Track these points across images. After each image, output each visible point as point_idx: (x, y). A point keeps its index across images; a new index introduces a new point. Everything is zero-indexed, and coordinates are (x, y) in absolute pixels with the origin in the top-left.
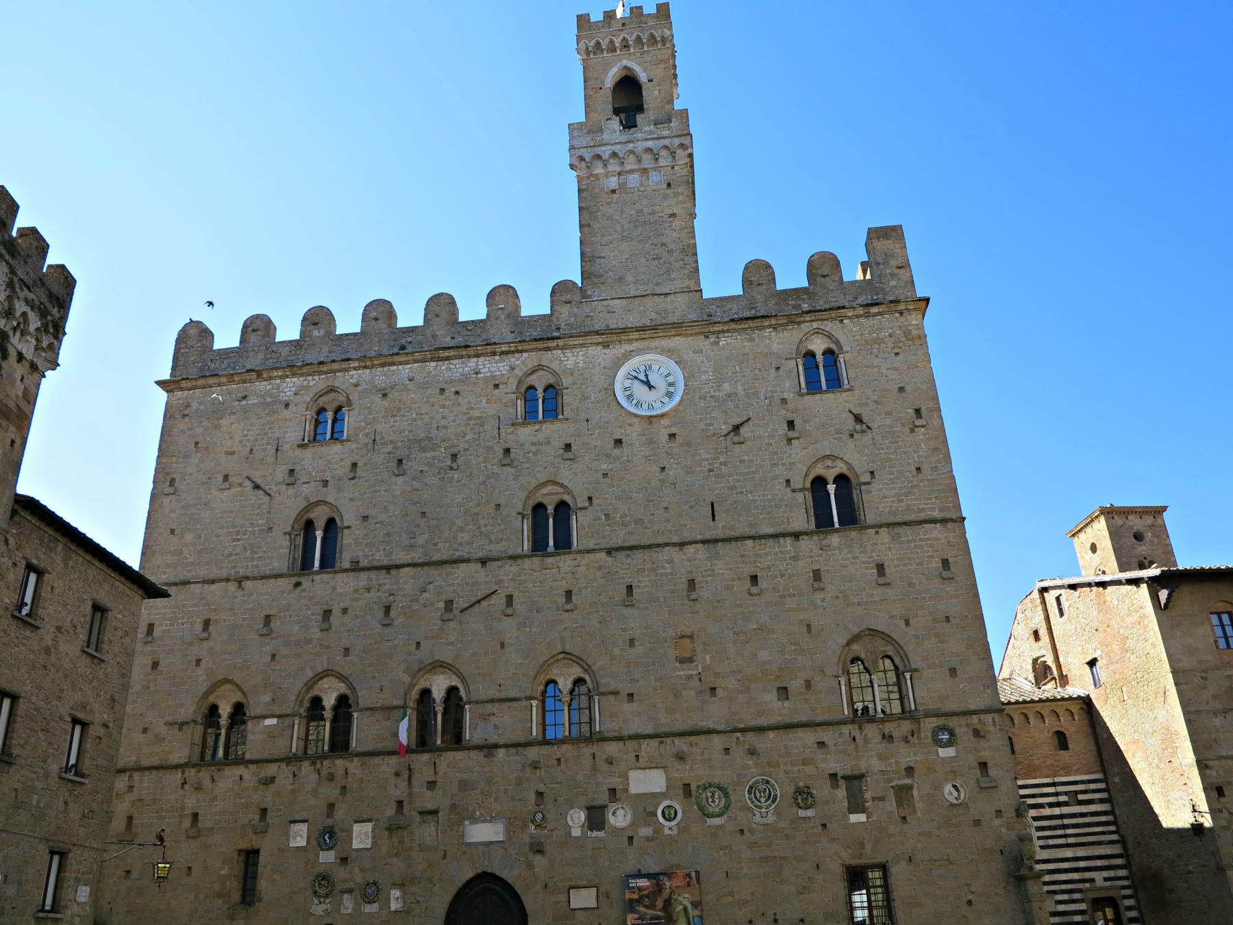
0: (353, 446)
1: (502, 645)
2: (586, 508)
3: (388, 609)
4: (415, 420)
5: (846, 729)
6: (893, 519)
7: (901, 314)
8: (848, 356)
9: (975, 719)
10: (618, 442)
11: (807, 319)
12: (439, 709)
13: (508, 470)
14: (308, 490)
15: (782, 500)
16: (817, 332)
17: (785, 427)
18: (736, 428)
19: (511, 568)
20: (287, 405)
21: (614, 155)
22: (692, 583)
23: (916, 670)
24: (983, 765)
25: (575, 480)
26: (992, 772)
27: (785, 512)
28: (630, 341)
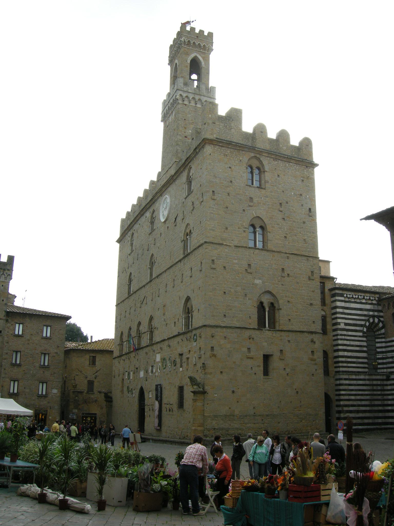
19: (147, 287)
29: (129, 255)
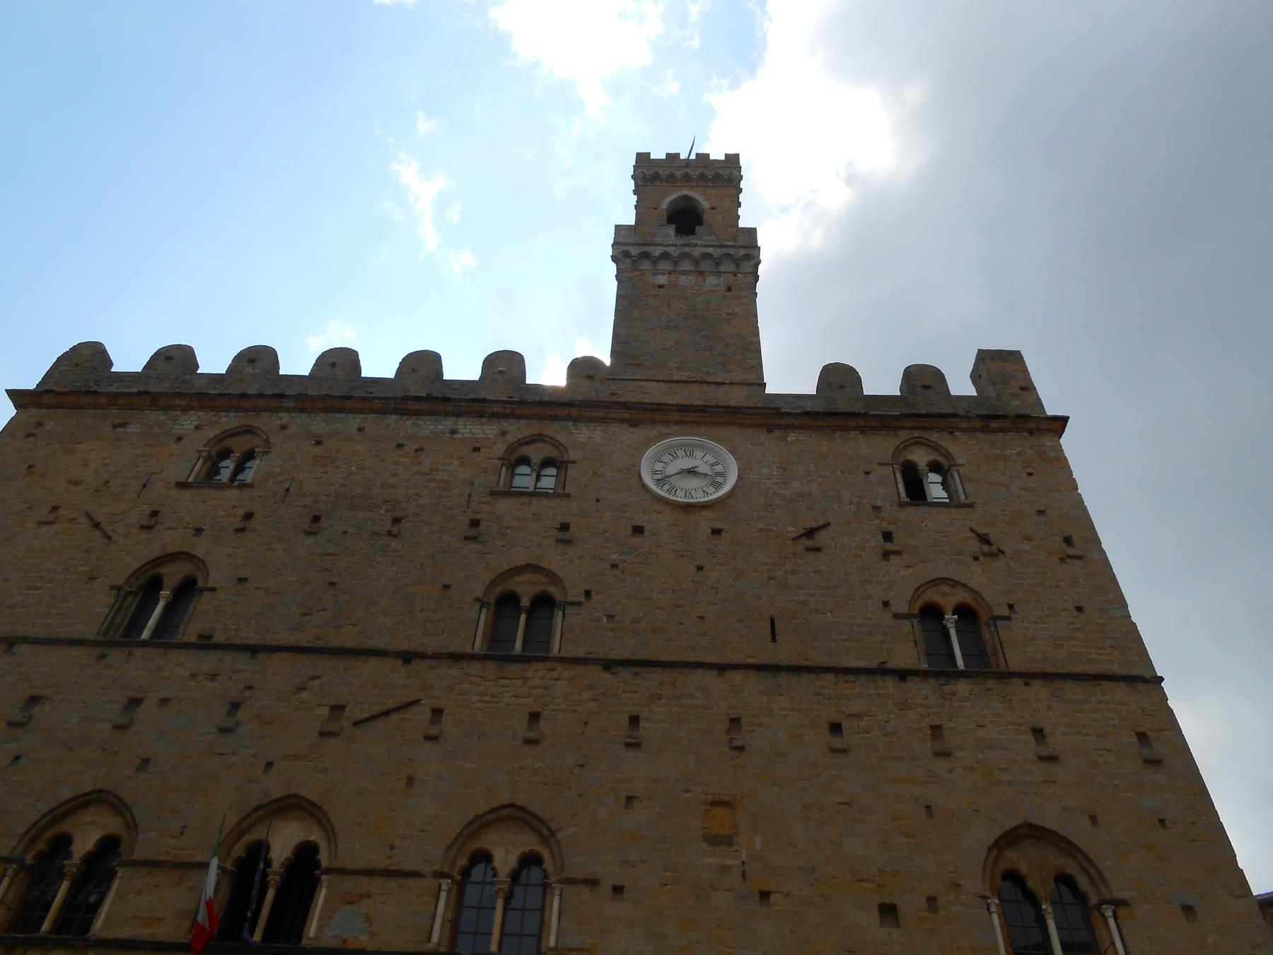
0: (255, 493)
1: (410, 781)
2: (579, 604)
3: (235, 707)
4: (352, 473)
6: (1049, 668)
7: (1031, 433)
8: (962, 470)
10: (638, 530)
11: (907, 424)
12: (274, 879)
13: (474, 546)
14: (168, 539)
16: (918, 442)
17: (880, 537)
18: (810, 533)
19: (452, 672)
20: (180, 439)
21: (665, 256)
22: (735, 722)
25: (571, 568)
28: (666, 423)
29: (182, 485)
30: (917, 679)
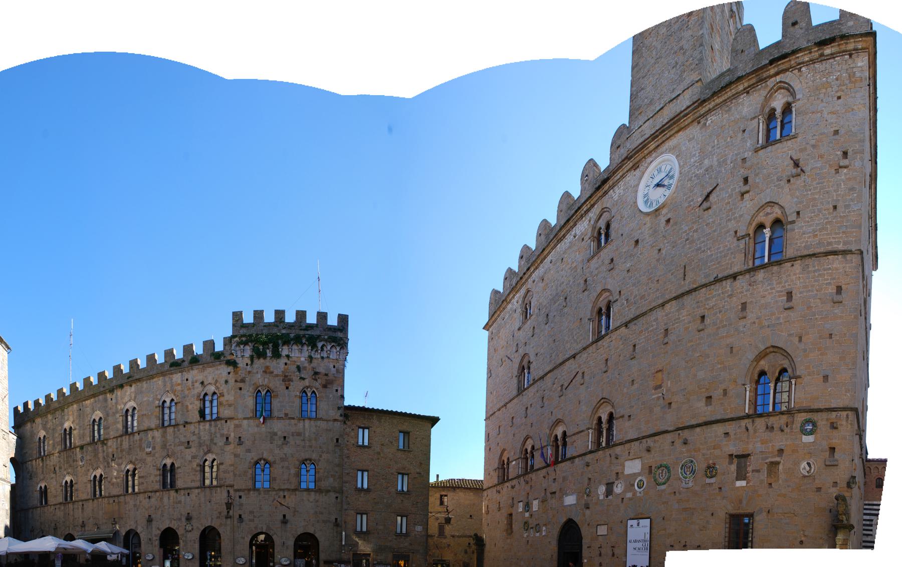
5: (743, 423)
6: (806, 252)
9: (834, 414)
15: (730, 249)
17: (741, 184)
23: (799, 377)
24: (833, 449)
26: (837, 455)
27: (730, 259)
30: (740, 277)
